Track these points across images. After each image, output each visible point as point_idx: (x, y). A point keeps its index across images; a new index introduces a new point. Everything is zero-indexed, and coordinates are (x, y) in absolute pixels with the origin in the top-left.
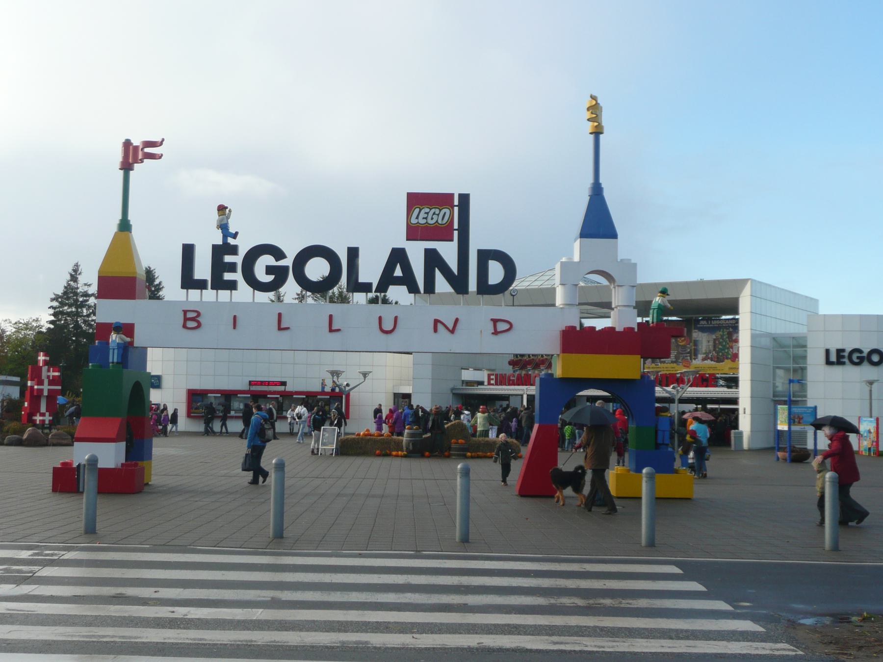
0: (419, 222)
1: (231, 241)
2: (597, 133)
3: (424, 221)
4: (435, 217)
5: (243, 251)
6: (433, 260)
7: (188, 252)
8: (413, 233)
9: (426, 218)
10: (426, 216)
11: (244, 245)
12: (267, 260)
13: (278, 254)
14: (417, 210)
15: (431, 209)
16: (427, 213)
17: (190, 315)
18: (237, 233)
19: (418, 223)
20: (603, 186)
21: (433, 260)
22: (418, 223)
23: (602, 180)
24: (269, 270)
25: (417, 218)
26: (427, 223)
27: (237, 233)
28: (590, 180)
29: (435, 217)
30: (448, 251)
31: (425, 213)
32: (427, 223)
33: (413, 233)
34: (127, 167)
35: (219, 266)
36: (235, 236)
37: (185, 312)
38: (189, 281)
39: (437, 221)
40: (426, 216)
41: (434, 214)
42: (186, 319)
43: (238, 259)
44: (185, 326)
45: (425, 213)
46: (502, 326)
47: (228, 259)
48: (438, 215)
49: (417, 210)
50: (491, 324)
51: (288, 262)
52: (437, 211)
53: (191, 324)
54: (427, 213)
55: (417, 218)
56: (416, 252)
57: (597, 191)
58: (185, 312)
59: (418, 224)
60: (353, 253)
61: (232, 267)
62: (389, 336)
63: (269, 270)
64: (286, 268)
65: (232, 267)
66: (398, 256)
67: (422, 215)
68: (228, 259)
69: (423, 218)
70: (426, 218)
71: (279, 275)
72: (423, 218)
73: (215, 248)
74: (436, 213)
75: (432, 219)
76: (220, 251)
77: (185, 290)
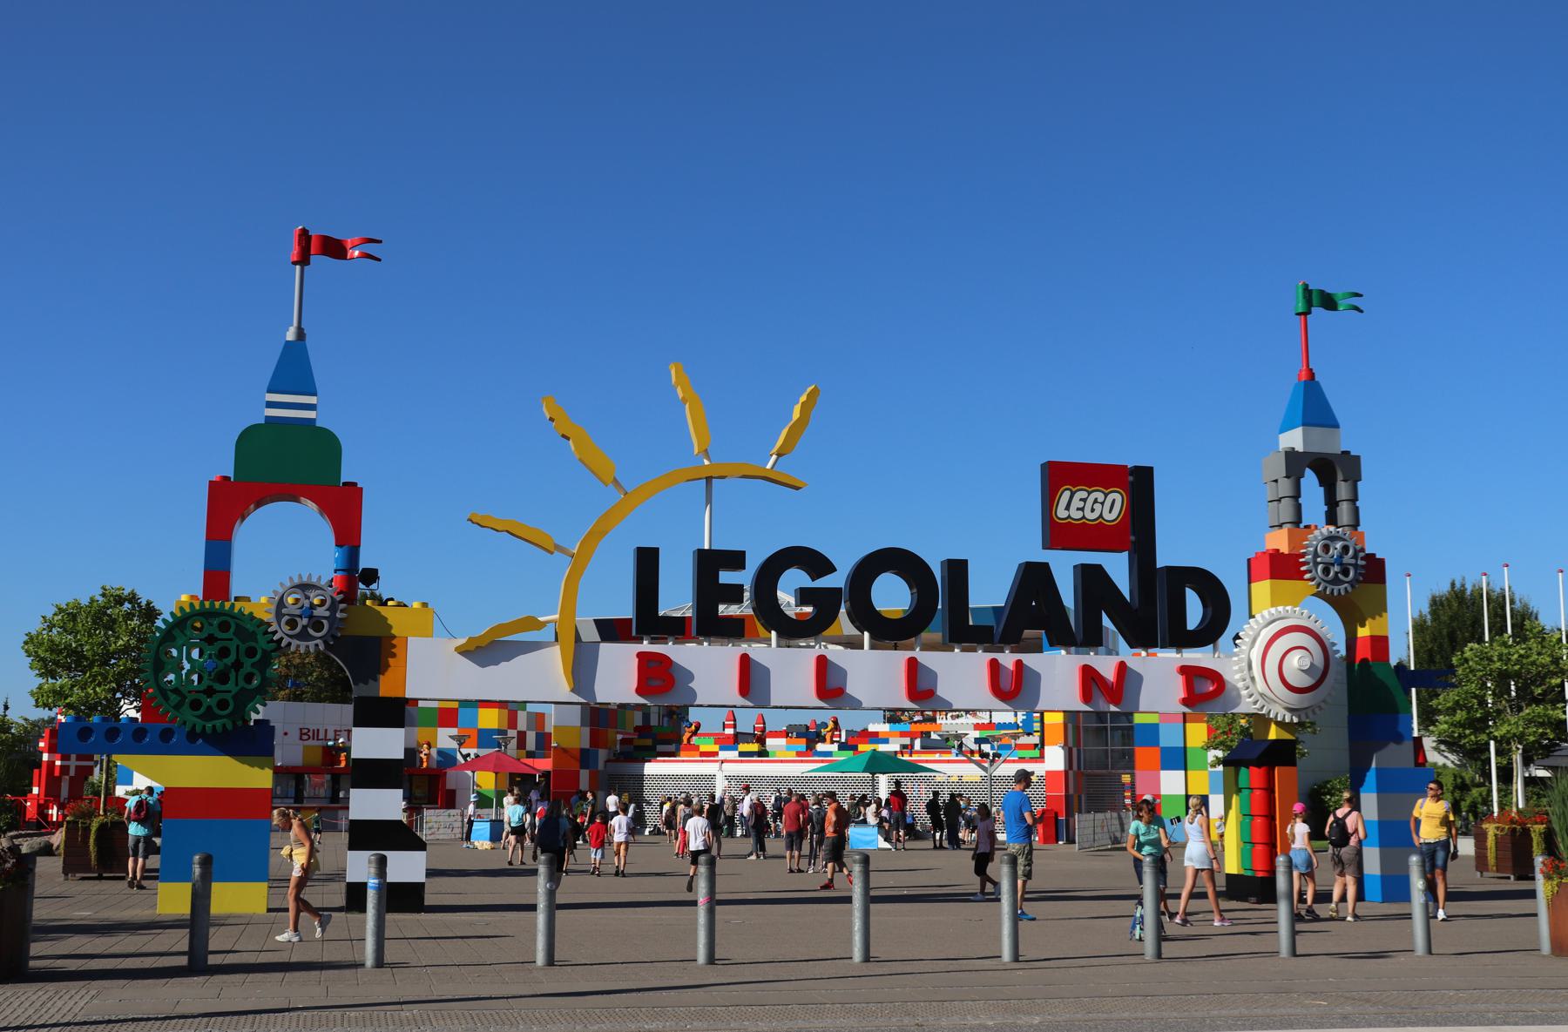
0: (1086, 516)
3: (1079, 515)
4: (1098, 507)
5: (753, 563)
6: (1091, 579)
8: (1060, 535)
9: (1082, 509)
10: (1081, 504)
13: (817, 564)
14: (1067, 494)
15: (1089, 493)
16: (1084, 500)
19: (1069, 517)
21: (1091, 579)
22: (1069, 517)
24: (804, 596)
25: (1068, 508)
26: (1084, 517)
29: (1098, 507)
30: (1117, 566)
31: (1081, 500)
32: (1084, 517)
33: (1060, 535)
35: (709, 591)
39: (1101, 516)
40: (1081, 504)
41: (1096, 501)
43: (744, 578)
45: (1081, 500)
47: (726, 577)
48: (1103, 503)
49: (1067, 494)
51: (836, 580)
52: (1100, 497)
54: (1084, 500)
55: (1068, 508)
56: (1064, 566)
59: (1069, 520)
60: (957, 570)
61: (734, 594)
63: (804, 596)
64: (835, 593)
65: (734, 594)
66: (1034, 579)
67: (1076, 503)
68: (726, 577)
69: (1078, 509)
70: (1082, 509)
71: (824, 604)
72: (1078, 509)
74: (1099, 500)
75: (1093, 510)
76: (710, 563)
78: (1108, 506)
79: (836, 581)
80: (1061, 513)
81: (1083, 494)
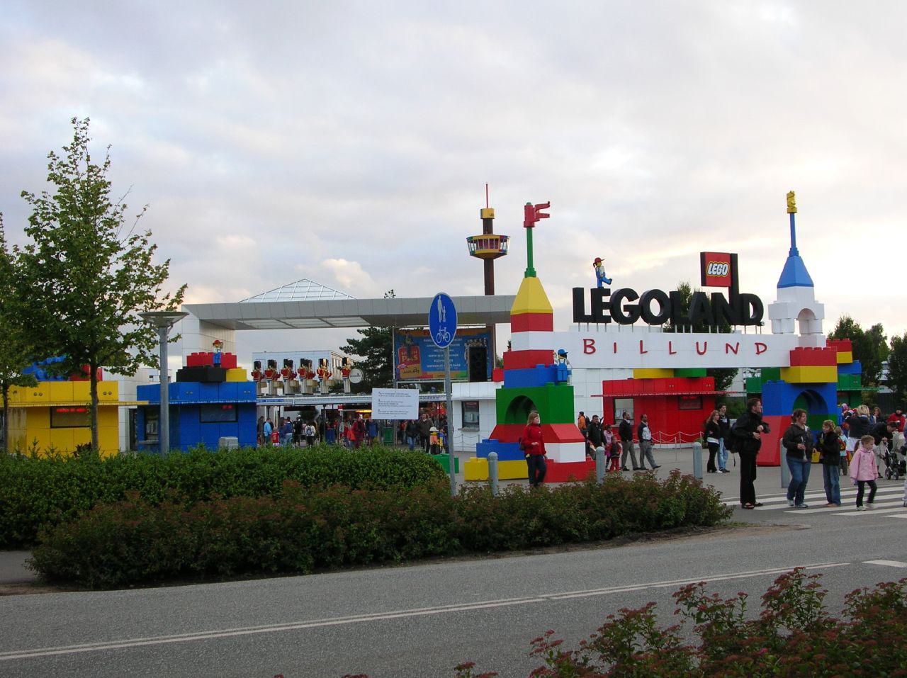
1: (605, 286)
2: (792, 214)
3: (714, 273)
7: (578, 293)
11: (614, 288)
12: (625, 301)
13: (631, 294)
17: (589, 343)
18: (611, 280)
20: (798, 250)
23: (798, 246)
27: (611, 280)
28: (789, 246)
34: (529, 224)
36: (609, 282)
37: (585, 340)
38: (579, 316)
42: (586, 346)
44: (585, 352)
46: (761, 348)
50: (756, 346)
53: (589, 350)
57: (794, 252)
58: (585, 340)
62: (703, 356)
67: (714, 269)
70: (715, 271)
73: (593, 291)
76: (597, 293)
77: (577, 323)
78: (722, 270)
79: (636, 302)
80: (709, 272)
81: (716, 265)
